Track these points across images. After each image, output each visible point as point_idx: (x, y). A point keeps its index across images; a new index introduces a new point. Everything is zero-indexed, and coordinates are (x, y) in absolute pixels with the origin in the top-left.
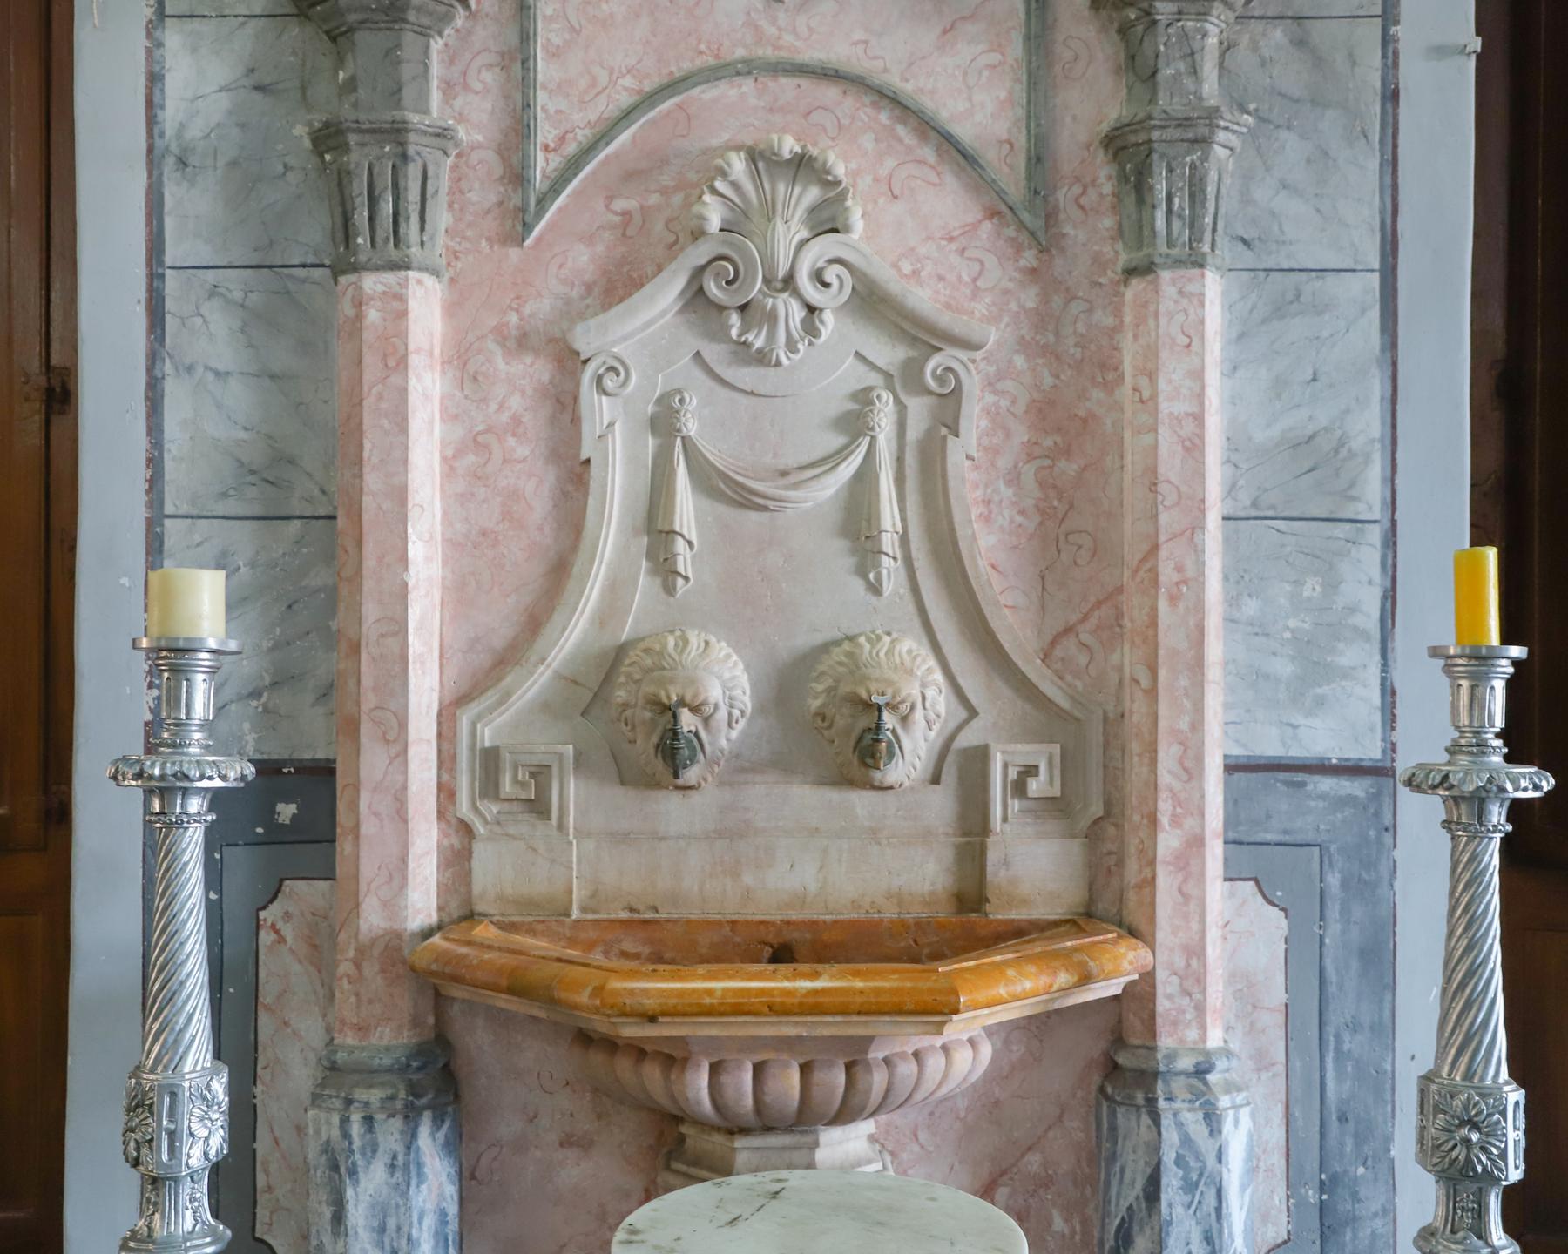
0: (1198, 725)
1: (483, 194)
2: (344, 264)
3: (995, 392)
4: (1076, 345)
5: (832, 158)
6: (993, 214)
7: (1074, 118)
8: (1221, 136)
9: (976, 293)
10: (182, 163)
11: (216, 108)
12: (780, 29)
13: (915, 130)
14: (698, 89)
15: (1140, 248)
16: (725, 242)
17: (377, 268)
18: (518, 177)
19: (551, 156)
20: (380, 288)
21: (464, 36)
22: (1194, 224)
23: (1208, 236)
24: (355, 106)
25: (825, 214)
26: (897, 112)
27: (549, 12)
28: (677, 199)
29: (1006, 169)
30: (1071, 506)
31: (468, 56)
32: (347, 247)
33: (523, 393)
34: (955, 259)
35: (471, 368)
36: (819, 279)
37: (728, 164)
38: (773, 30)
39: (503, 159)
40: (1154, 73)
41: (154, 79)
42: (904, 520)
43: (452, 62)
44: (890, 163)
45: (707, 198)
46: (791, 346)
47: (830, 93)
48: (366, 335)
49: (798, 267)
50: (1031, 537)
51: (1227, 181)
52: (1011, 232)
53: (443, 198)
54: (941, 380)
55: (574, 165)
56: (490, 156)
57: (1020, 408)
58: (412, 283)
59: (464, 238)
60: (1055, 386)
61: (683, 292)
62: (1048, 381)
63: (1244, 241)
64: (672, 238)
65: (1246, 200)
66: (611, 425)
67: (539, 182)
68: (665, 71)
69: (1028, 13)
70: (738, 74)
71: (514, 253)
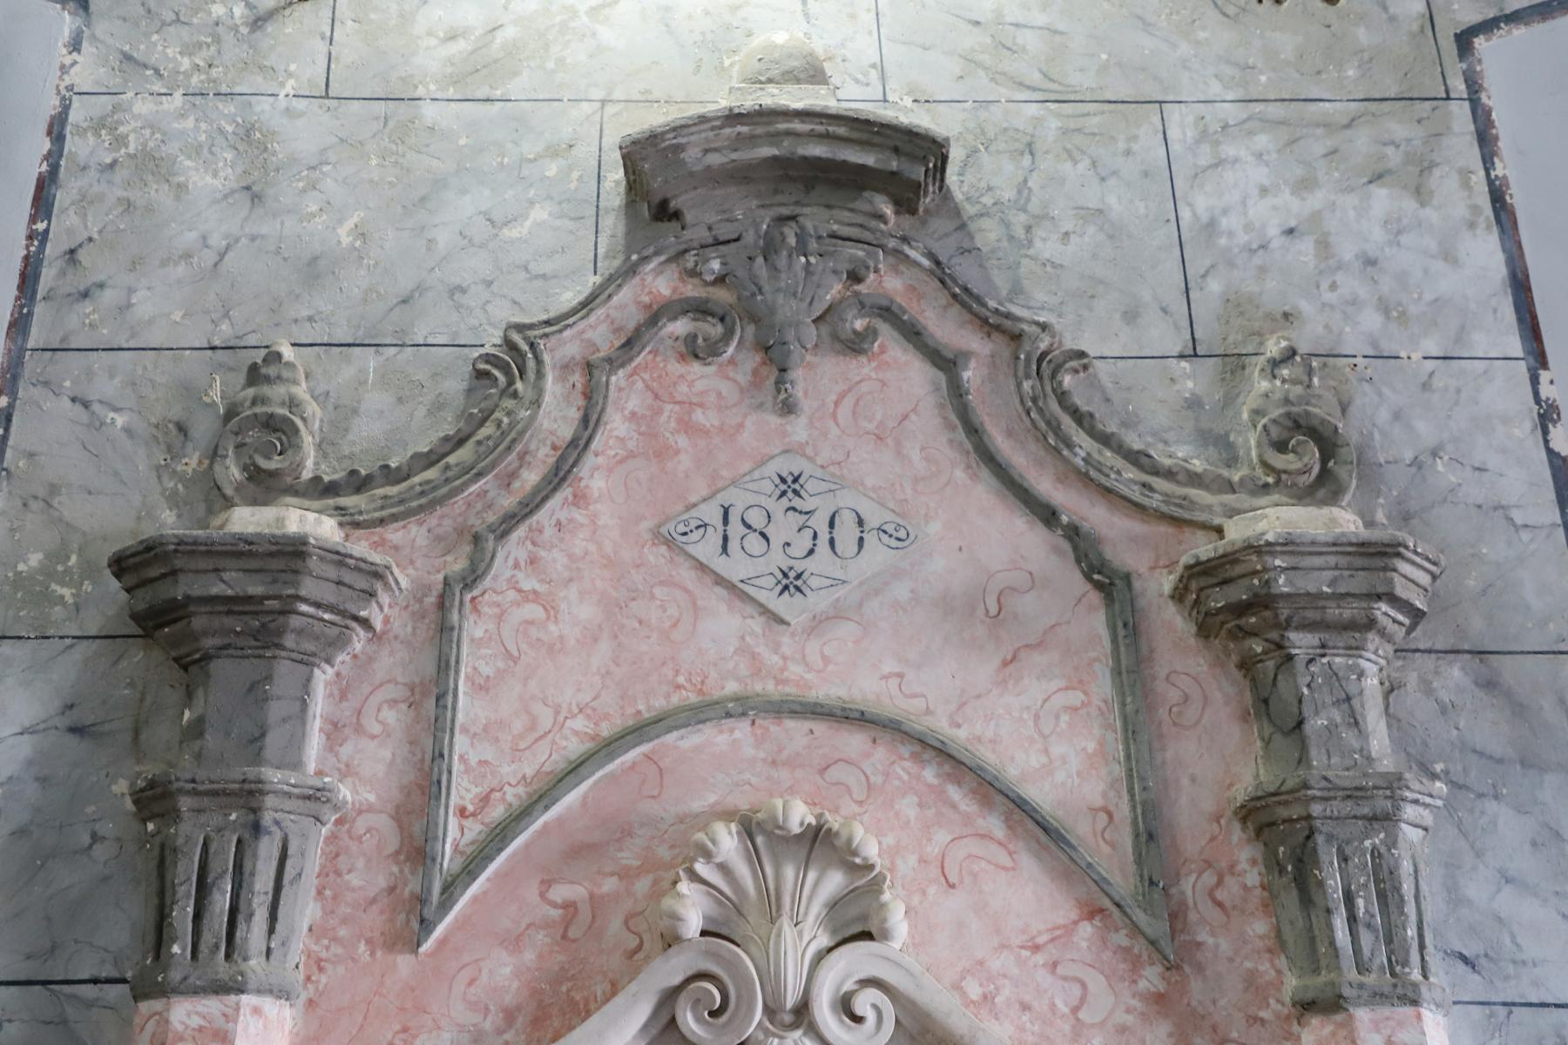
1: (367, 876)
2: (150, 984)
5: (859, 833)
6: (1092, 912)
7: (1193, 780)
8: (1410, 811)
12: (784, 658)
13: (974, 792)
14: (675, 734)
15: (1316, 971)
16: (709, 954)
17: (196, 991)
19: (467, 823)
20: (196, 1021)
21: (363, 663)
22: (1390, 937)
23: (1415, 957)
24: (198, 756)
25: (853, 911)
26: (947, 768)
27: (479, 633)
28: (642, 885)
29: (1106, 849)
31: (366, 689)
32: (157, 957)
36: (846, 1008)
37: (714, 842)
38: (776, 659)
39: (401, 827)
40: (1300, 724)
43: (343, 696)
44: (942, 837)
45: (684, 887)
47: (854, 741)
49: (815, 991)
51: (1424, 872)
52: (1121, 938)
53: (310, 881)
55: (500, 836)
56: (383, 822)
58: (245, 1011)
61: (646, 1027)
63: (1464, 959)
64: (633, 942)
65: (1455, 898)
67: (448, 858)
68: (630, 711)
69: (1114, 640)
70: (729, 715)
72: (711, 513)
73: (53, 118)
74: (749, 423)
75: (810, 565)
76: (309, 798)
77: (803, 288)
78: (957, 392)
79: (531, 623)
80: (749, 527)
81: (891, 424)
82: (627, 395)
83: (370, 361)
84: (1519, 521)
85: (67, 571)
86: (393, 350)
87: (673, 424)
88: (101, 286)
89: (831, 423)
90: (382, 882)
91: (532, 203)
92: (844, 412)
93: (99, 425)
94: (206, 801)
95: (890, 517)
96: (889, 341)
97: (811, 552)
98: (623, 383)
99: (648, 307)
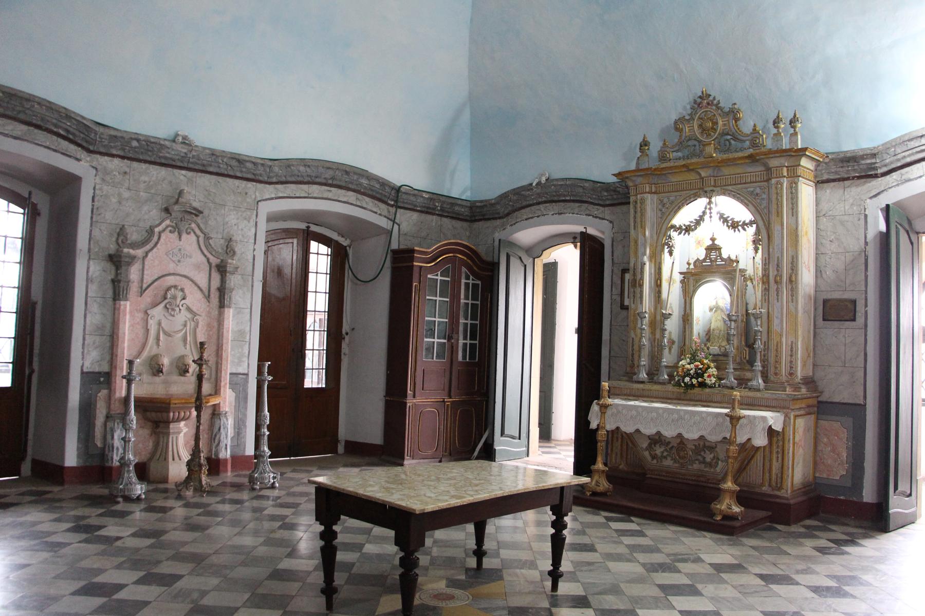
11: (97, 273)
18: (141, 287)
41: (88, 268)
47: (184, 279)
77: (183, 226)
78: (198, 241)
82: (163, 236)
96: (192, 233)
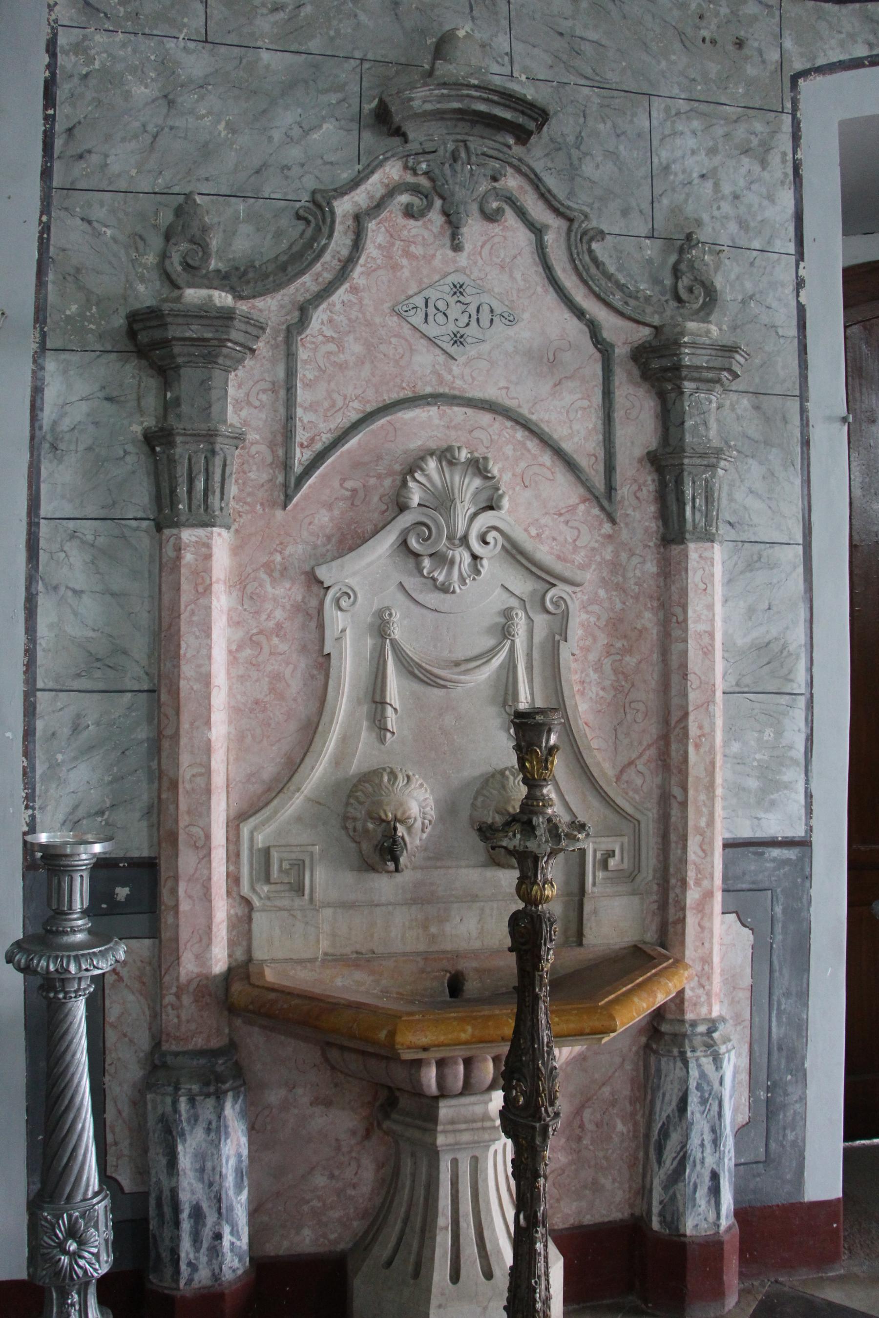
0: (711, 823)
1: (258, 475)
3: (587, 612)
4: (636, 584)
9: (576, 549)
10: (54, 447)
19: (304, 451)
26: (527, 433)
27: (305, 357)
30: (633, 685)
33: (284, 607)
34: (562, 527)
35: (249, 589)
38: (450, 377)
39: (273, 452)
41: (37, 391)
42: (532, 694)
46: (463, 580)
47: (486, 418)
48: (183, 570)
50: (609, 704)
54: (556, 604)
56: (263, 448)
57: (602, 623)
59: (245, 503)
60: (623, 609)
62: (619, 606)
66: (343, 630)
71: (279, 514)
72: (419, 301)
73: (48, 41)
74: (438, 253)
75: (467, 331)
76: (236, 438)
79: (331, 353)
80: (438, 309)
81: (508, 260)
82: (376, 234)
83: (241, 206)
84: (781, 334)
85: (92, 315)
86: (252, 200)
87: (400, 252)
88: (89, 152)
89: (479, 258)
90: (265, 477)
91: (324, 119)
92: (485, 251)
93: (98, 235)
94: (189, 439)
95: (506, 309)
97: (468, 324)
98: (374, 228)
99: (387, 186)
